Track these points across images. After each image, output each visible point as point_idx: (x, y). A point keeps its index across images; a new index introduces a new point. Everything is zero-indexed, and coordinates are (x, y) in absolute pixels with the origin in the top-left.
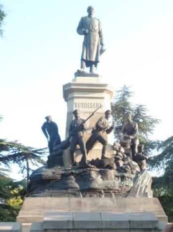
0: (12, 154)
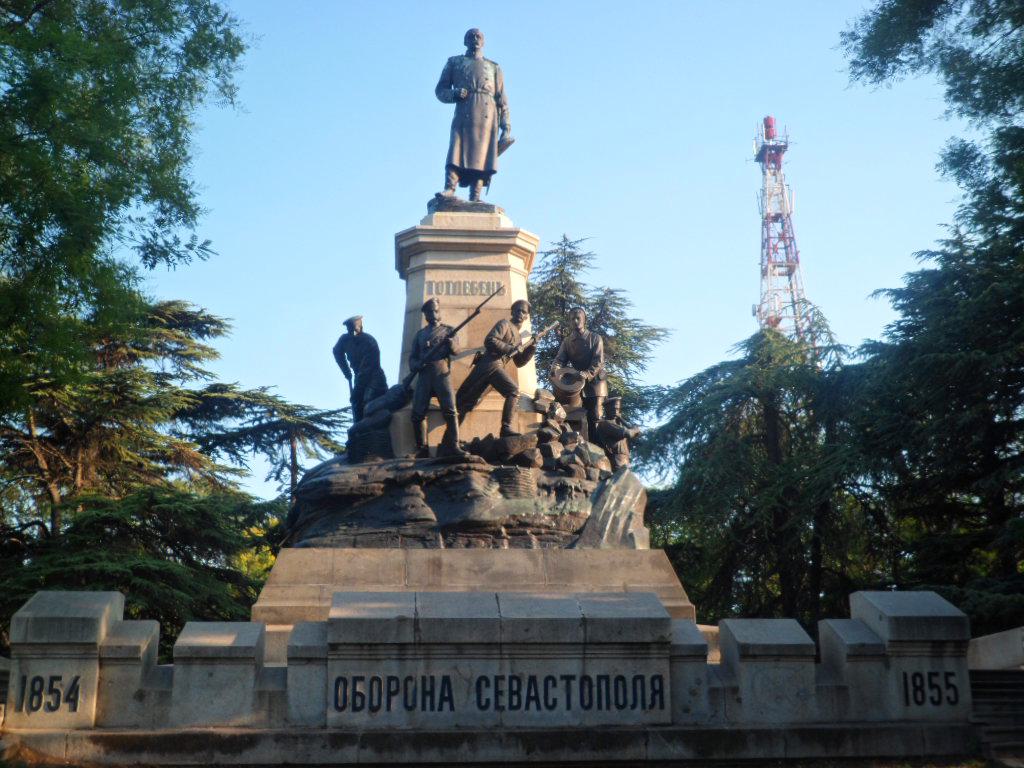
0: (250, 425)
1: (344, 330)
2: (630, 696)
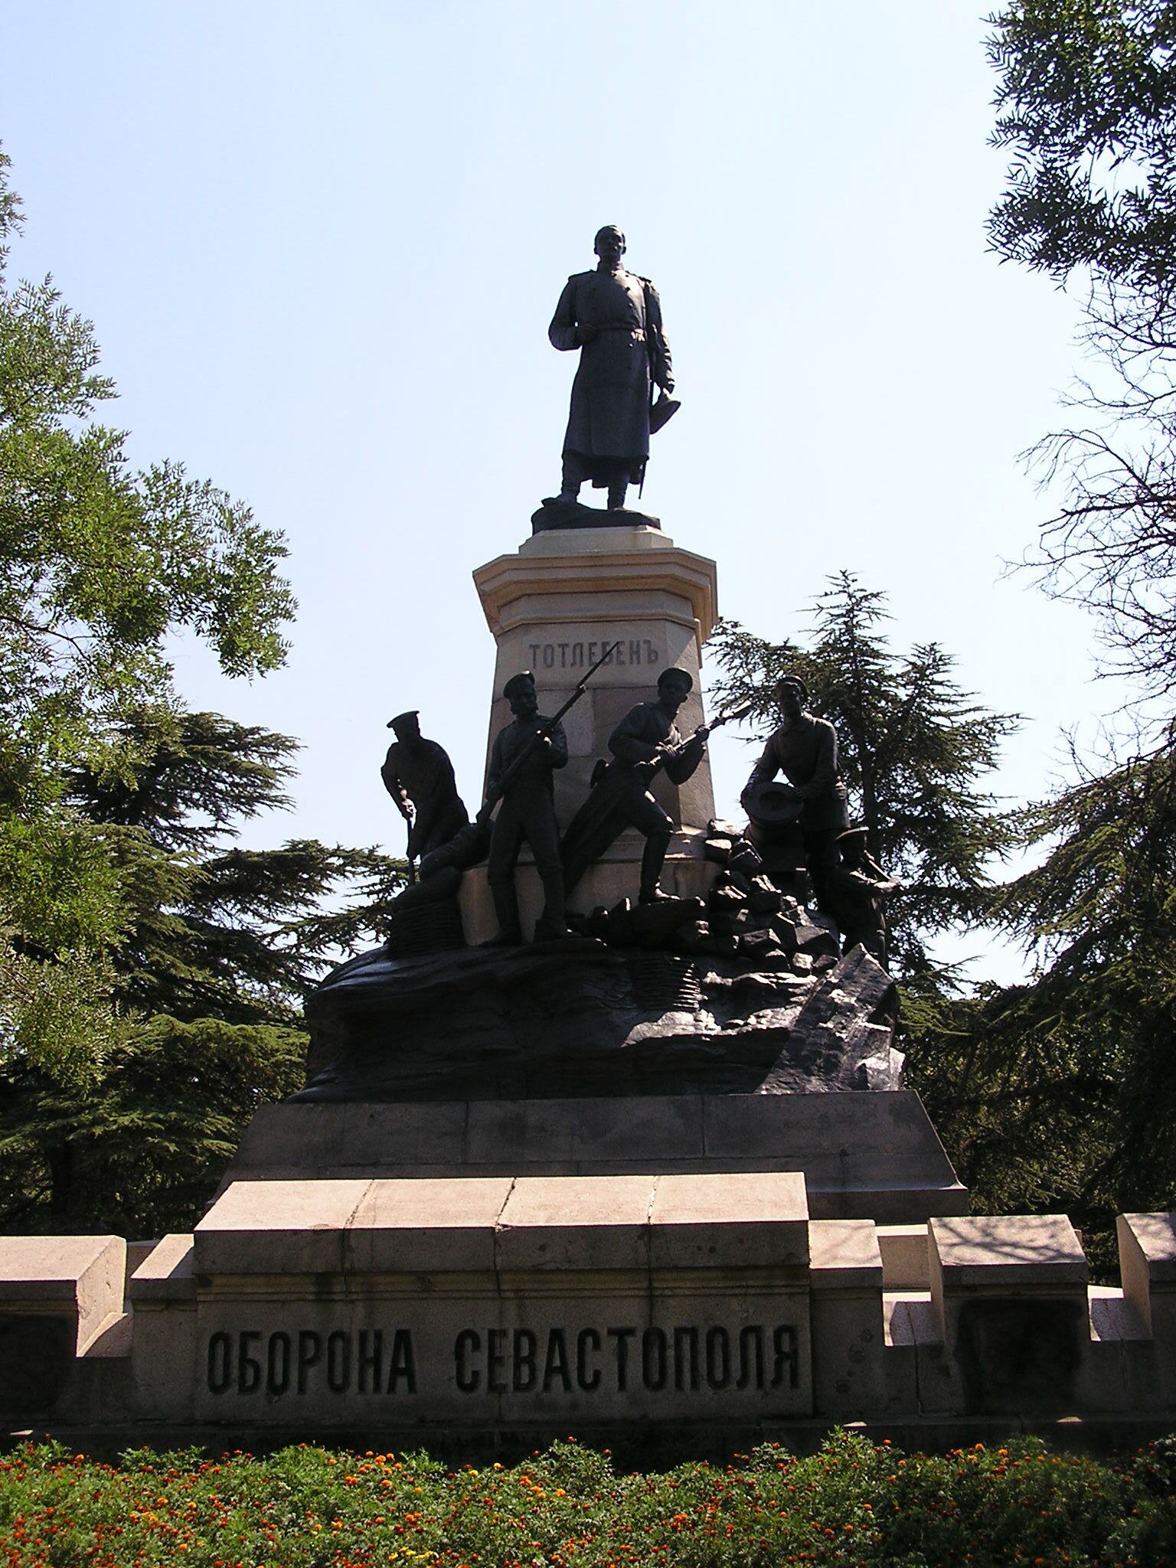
1: (391, 738)
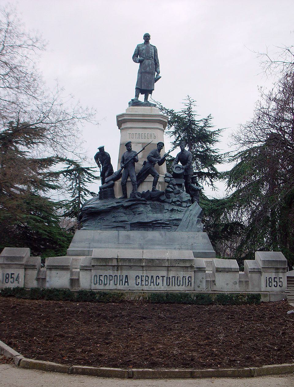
2: (181, 282)
